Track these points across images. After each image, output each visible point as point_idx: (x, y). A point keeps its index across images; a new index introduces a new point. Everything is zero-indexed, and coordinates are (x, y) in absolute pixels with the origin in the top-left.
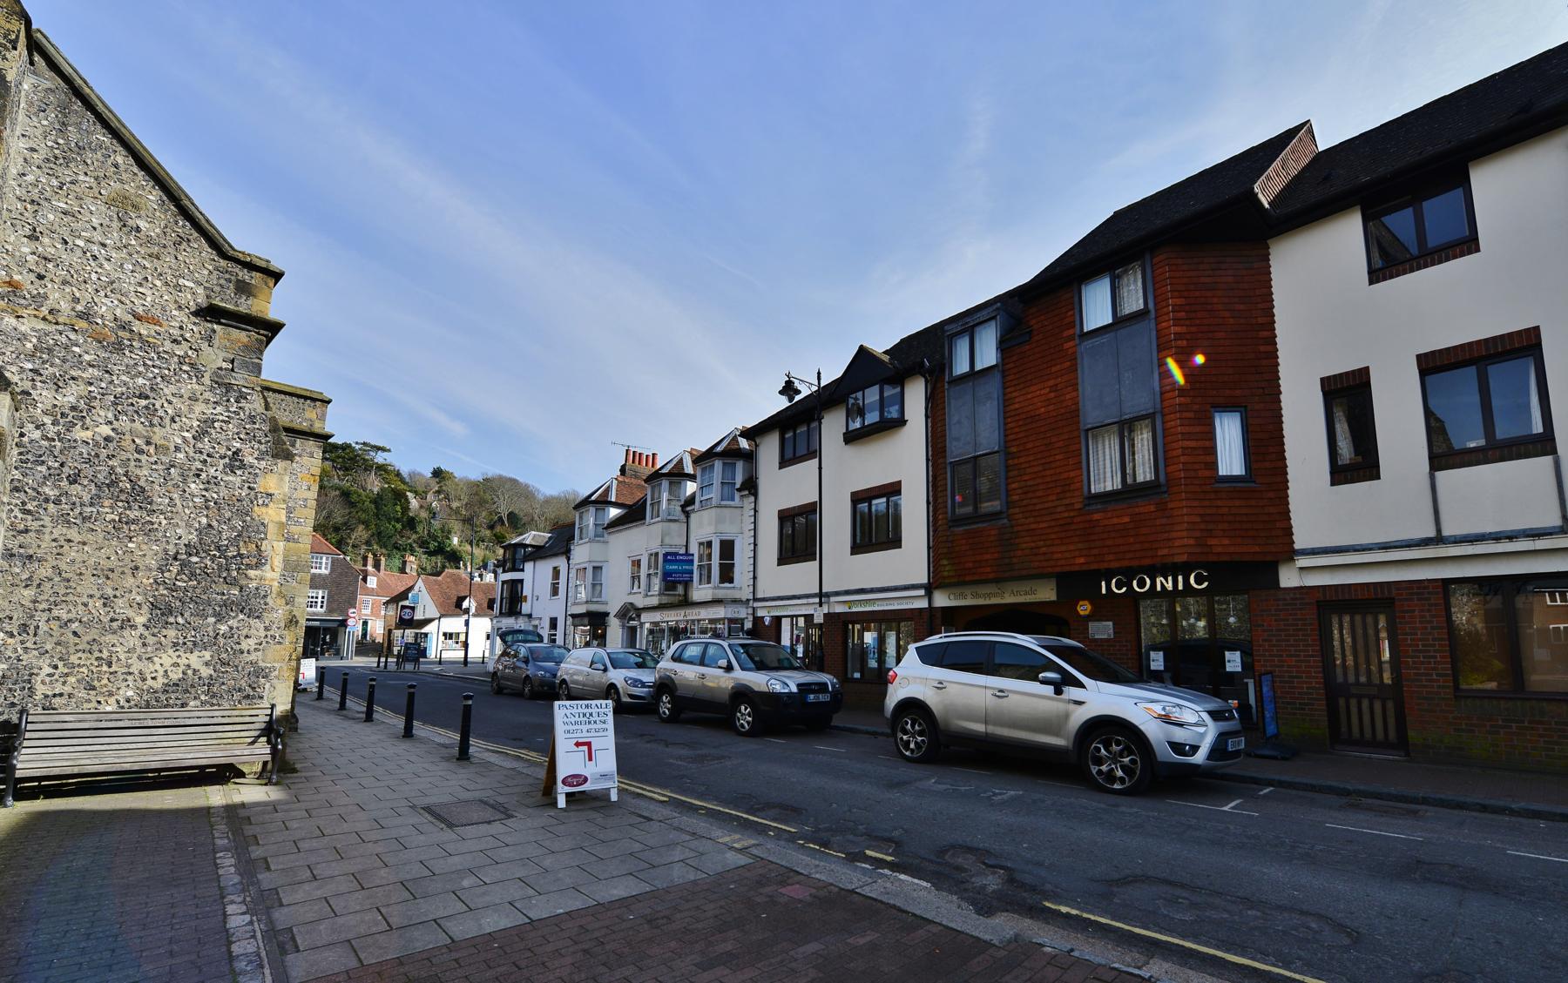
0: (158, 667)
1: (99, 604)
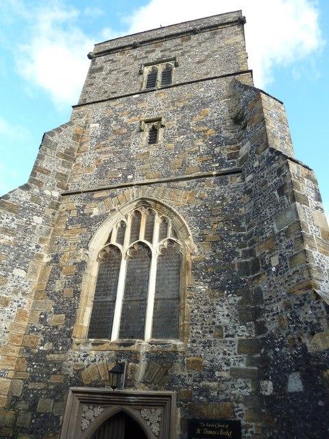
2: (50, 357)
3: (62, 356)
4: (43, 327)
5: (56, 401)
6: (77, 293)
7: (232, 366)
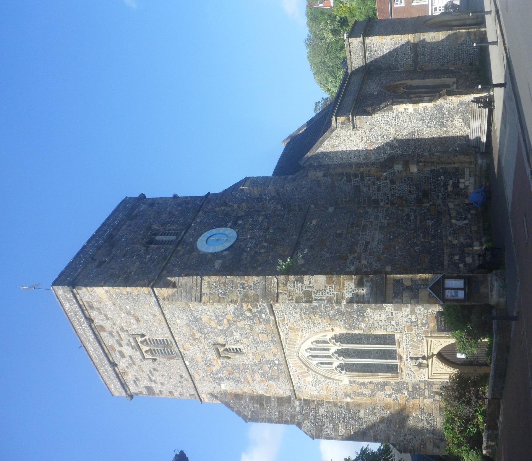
0: (458, 124)
2: (410, 390)
4: (393, 395)
5: (434, 384)
6: (371, 383)
7: (409, 314)
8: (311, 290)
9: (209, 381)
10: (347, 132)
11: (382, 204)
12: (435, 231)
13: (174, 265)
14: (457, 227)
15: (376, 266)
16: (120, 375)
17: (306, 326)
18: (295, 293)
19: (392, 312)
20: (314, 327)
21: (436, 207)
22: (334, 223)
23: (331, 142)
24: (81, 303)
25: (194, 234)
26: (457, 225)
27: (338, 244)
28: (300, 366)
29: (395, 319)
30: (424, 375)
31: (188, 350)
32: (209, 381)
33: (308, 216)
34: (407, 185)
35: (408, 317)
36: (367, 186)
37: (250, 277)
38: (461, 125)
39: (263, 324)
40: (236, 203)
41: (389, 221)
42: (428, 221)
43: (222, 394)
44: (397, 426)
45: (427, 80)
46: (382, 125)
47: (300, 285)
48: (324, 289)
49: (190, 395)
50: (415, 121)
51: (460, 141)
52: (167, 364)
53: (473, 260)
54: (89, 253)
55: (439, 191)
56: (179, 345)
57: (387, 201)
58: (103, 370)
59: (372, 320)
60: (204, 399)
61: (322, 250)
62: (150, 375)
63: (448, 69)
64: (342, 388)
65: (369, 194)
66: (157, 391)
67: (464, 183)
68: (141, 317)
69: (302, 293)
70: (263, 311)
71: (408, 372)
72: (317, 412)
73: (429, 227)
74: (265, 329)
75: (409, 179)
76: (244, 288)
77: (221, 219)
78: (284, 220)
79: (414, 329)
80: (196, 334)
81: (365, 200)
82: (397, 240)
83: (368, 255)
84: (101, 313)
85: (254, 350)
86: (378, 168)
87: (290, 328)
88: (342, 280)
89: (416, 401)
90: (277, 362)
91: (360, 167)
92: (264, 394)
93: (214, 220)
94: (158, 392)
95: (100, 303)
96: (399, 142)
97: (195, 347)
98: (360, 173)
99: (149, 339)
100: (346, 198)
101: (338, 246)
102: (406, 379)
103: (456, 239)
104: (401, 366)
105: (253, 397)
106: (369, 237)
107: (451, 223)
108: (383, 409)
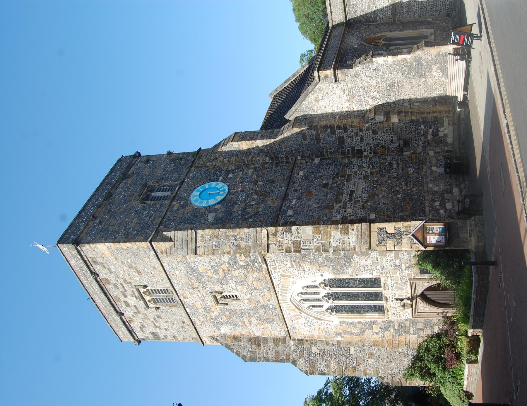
1: (420, 87)
2: (396, 327)
3: (396, 323)
4: (381, 333)
5: (418, 322)
6: (359, 322)
7: (393, 259)
8: (299, 240)
9: (209, 326)
10: (329, 85)
11: (365, 154)
12: (416, 179)
13: (170, 220)
14: (437, 173)
15: (361, 214)
16: (127, 323)
17: (297, 273)
18: (284, 244)
19: (377, 257)
20: (305, 274)
21: (417, 155)
22: (320, 174)
23: (314, 96)
24: (86, 259)
25: (188, 189)
26: (437, 172)
27: (325, 194)
28: (292, 310)
29: (380, 264)
30: (409, 314)
31: (187, 299)
32: (209, 326)
33: (294, 168)
34: (389, 135)
35: (392, 262)
36: (350, 137)
37: (242, 229)
38: (439, 76)
39: (256, 272)
40: (226, 157)
41: (373, 170)
42: (409, 169)
43: (222, 337)
44: (385, 361)
45: (406, 32)
46: (363, 78)
47: (289, 235)
48: (311, 238)
49: (192, 339)
50: (395, 73)
51: (438, 91)
52: (169, 311)
53: (453, 206)
54: (90, 211)
55: (419, 140)
56: (179, 294)
57: (370, 151)
58: (111, 319)
59: (359, 265)
60: (205, 342)
61: (309, 200)
62: (155, 322)
63: (426, 20)
64: (333, 328)
65: (353, 144)
66: (162, 336)
67: (443, 131)
68: (142, 269)
69: (291, 243)
70: (256, 260)
71: (394, 312)
72: (310, 350)
73: (410, 175)
74: (259, 277)
75: (391, 129)
76: (236, 240)
77: (212, 173)
78: (273, 173)
79: (398, 273)
80: (194, 284)
81: (349, 150)
82: (380, 188)
83: (353, 204)
84: (105, 267)
85: (249, 296)
86: (360, 119)
87: (282, 275)
88: (328, 230)
89: (402, 338)
90: (271, 307)
91: (343, 119)
92: (261, 335)
93: (206, 175)
94: (163, 337)
95: (103, 258)
96: (379, 94)
97: (194, 296)
98: (344, 125)
99: (151, 290)
100: (331, 149)
101: (324, 196)
102: (391, 317)
103: (437, 186)
104: (387, 307)
105: (251, 338)
106: (354, 186)
107: (431, 170)
108: (371, 346)
